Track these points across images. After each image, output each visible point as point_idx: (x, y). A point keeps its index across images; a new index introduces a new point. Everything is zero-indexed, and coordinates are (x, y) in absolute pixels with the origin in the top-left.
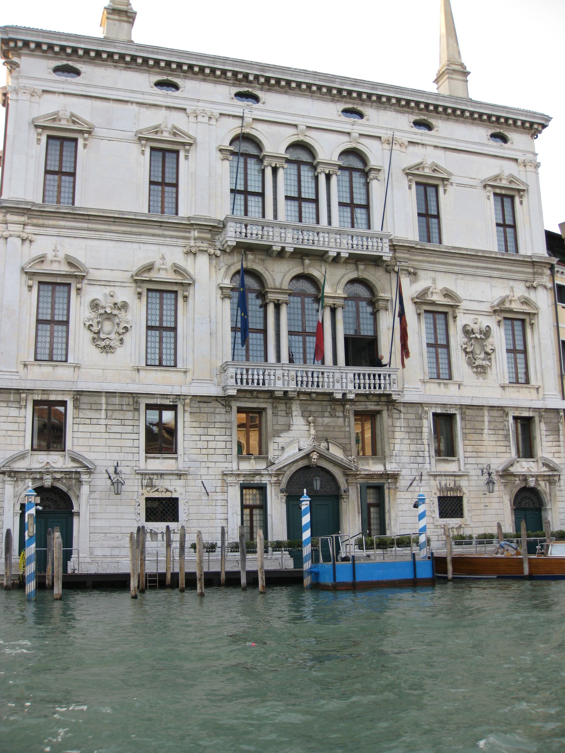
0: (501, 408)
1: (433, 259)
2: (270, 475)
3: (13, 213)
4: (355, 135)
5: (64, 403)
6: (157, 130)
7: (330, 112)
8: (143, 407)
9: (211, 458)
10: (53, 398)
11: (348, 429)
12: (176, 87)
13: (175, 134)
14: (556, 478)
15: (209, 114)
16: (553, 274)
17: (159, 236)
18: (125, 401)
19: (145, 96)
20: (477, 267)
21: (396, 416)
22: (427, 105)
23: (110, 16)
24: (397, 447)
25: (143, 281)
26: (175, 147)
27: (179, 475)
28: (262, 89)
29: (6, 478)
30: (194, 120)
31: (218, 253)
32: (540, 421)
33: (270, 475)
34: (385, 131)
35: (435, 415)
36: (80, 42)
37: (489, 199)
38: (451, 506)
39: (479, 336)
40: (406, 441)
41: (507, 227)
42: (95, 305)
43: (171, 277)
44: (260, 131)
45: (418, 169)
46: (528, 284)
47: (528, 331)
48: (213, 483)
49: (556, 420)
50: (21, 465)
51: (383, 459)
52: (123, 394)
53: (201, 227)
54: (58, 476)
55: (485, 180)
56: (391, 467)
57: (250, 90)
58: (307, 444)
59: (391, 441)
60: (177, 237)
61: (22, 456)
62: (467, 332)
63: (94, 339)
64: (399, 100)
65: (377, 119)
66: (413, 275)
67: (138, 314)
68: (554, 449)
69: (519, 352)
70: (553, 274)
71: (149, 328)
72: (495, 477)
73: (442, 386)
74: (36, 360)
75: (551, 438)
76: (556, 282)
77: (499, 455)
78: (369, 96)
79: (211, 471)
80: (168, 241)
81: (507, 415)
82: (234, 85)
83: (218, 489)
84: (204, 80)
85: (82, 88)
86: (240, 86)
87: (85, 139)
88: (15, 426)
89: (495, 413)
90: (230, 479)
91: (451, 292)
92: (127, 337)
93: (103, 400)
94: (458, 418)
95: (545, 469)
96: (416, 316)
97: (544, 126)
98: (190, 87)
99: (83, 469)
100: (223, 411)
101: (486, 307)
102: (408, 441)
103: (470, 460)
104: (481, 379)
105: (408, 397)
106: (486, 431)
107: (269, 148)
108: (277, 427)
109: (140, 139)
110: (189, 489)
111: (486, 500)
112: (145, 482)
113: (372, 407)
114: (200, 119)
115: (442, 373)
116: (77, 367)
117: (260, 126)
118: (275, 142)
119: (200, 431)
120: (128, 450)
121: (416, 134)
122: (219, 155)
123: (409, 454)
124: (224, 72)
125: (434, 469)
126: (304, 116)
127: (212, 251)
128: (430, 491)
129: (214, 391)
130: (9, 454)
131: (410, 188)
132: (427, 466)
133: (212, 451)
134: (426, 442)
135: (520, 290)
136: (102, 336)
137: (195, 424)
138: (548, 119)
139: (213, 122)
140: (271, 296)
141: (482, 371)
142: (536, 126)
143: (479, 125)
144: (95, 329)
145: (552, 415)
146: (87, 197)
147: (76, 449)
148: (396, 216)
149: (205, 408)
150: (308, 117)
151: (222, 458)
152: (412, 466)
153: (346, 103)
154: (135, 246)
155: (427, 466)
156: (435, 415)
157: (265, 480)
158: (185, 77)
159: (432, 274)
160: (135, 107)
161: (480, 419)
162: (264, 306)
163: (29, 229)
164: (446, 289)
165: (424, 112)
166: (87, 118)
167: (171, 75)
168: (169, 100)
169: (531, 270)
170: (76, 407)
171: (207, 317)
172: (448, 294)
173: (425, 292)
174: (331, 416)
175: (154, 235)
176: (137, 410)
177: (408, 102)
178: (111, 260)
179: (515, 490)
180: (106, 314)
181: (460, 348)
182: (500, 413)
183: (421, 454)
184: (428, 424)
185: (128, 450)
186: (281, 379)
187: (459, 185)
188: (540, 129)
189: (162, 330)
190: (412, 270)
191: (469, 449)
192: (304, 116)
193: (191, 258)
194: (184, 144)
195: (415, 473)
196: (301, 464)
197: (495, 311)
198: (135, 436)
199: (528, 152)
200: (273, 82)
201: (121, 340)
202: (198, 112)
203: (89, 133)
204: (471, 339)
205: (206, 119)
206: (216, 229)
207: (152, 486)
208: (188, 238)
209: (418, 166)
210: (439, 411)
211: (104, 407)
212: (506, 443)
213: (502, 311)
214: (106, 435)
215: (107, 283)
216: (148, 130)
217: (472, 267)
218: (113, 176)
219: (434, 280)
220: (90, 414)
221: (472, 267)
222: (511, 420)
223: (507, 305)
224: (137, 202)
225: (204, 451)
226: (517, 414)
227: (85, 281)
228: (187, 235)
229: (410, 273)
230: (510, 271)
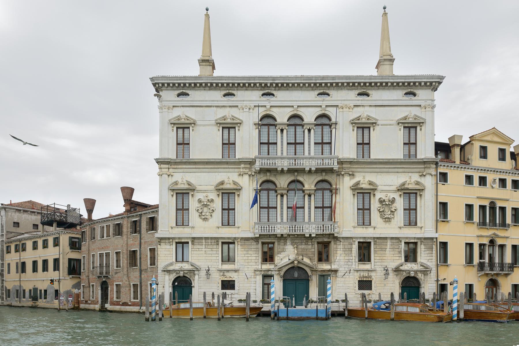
1: (363, 166)
2: (276, 271)
3: (163, 164)
4: (324, 106)
5: (188, 243)
6: (224, 118)
8: (220, 244)
9: (250, 264)
10: (183, 241)
11: (313, 250)
12: (233, 95)
13: (233, 119)
14: (429, 272)
15: (249, 107)
16: (437, 168)
17: (226, 168)
18: (213, 241)
19: (219, 102)
20: (389, 168)
21: (338, 243)
22: (365, 83)
23: (201, 64)
24: (338, 258)
25: (220, 189)
26: (234, 126)
27: (236, 271)
28: (275, 90)
29: (166, 273)
30: (242, 111)
31: (253, 173)
32: (421, 244)
33: (276, 271)
34: (340, 102)
35: (359, 242)
36: (186, 80)
37: (400, 130)
38: (365, 284)
39: (387, 203)
40: (343, 255)
41: (410, 144)
42: (200, 201)
43: (232, 186)
44: (275, 112)
45: (359, 120)
46: (420, 174)
47: (418, 198)
48: (250, 274)
49: (431, 243)
50: (171, 268)
51: (330, 264)
52: (212, 238)
53: (245, 163)
54: (186, 272)
55: (398, 120)
56: (334, 267)
57: (269, 91)
58: (292, 257)
59: (335, 255)
60: (235, 168)
61: (171, 264)
62: (381, 201)
63: (200, 215)
64: (348, 83)
65: (337, 96)
66: (352, 175)
67: (218, 204)
68: (428, 258)
70: (437, 168)
71: (223, 209)
72: (390, 271)
73: (364, 229)
74: (176, 225)
75: (427, 252)
76: (438, 171)
77: (395, 261)
78: (332, 84)
79: (249, 269)
80: (231, 170)
81: (401, 241)
82: (261, 90)
83: (252, 277)
84: (246, 90)
85: (190, 102)
86: (264, 90)
87: (193, 127)
88: (169, 253)
89: (394, 241)
90: (257, 273)
91: (372, 182)
92: (213, 214)
93: (204, 241)
94: (372, 244)
95: (422, 267)
96: (352, 196)
97: (440, 83)
98: (241, 95)
99: (195, 270)
100: (255, 243)
101: (394, 188)
102: (344, 255)
103: (377, 264)
104: (387, 224)
105: (344, 235)
106: (388, 250)
107: (279, 120)
108: (280, 250)
109: (217, 123)
110: (239, 276)
111: (385, 282)
112: (221, 274)
113: (326, 240)
114: (245, 110)
116: (193, 227)
117: (274, 109)
118: (282, 116)
119: (245, 252)
120: (214, 261)
121: (358, 100)
122: (255, 127)
123: (344, 261)
124: (255, 84)
125: (357, 268)
126: (296, 101)
127: (250, 173)
129: (251, 235)
130: (167, 263)
131: (353, 130)
132: (354, 266)
133: (250, 261)
134: (353, 255)
135: (415, 177)
136: (203, 214)
137: (242, 250)
138: (443, 78)
139: (251, 110)
140: (279, 192)
141: (388, 220)
142: (434, 84)
143: (397, 89)
144: (200, 211)
145: (429, 241)
146: (195, 154)
147: (193, 261)
148: (345, 145)
149: (247, 243)
150: (299, 101)
151: (254, 264)
152: (345, 266)
153: (320, 90)
154: (217, 174)
155: (354, 266)
156: (359, 242)
157: (273, 273)
158: (237, 90)
159: (364, 174)
160: (215, 108)
161: (385, 244)
162: (277, 196)
163: (171, 170)
164: (370, 181)
165: (363, 87)
166: (193, 117)
167: (230, 90)
168: (230, 102)
169: (423, 166)
170: (193, 244)
172: (371, 183)
173: (358, 183)
174: (306, 244)
175: (224, 168)
176: (218, 244)
177: (354, 83)
178: (205, 181)
179: (403, 278)
180: (205, 205)
181: (376, 209)
182: (397, 241)
183: (351, 261)
184: (355, 247)
185: (214, 261)
187: (382, 125)
188: (437, 84)
189: (228, 211)
190: (351, 173)
191: (377, 258)
192: (296, 101)
193: (241, 177)
194: (237, 123)
195: (347, 269)
196: (290, 266)
197: (398, 190)
198: (217, 255)
199: (428, 100)
200: (280, 85)
201: (211, 215)
202: (243, 107)
203: (194, 124)
204: (383, 205)
205: (248, 110)
206: (252, 163)
207: (224, 275)
208: (239, 168)
209: (358, 118)
210: (362, 240)
211: (204, 243)
212: (399, 255)
213: (402, 190)
214: (205, 255)
215: (205, 191)
216: (219, 119)
217: (387, 168)
218: (206, 143)
219: (364, 177)
220: (198, 247)
221: (387, 168)
222: (403, 244)
223: (406, 186)
225: (246, 261)
226: (407, 241)
227: (195, 191)
228: (239, 166)
229: (350, 175)
230: (410, 168)
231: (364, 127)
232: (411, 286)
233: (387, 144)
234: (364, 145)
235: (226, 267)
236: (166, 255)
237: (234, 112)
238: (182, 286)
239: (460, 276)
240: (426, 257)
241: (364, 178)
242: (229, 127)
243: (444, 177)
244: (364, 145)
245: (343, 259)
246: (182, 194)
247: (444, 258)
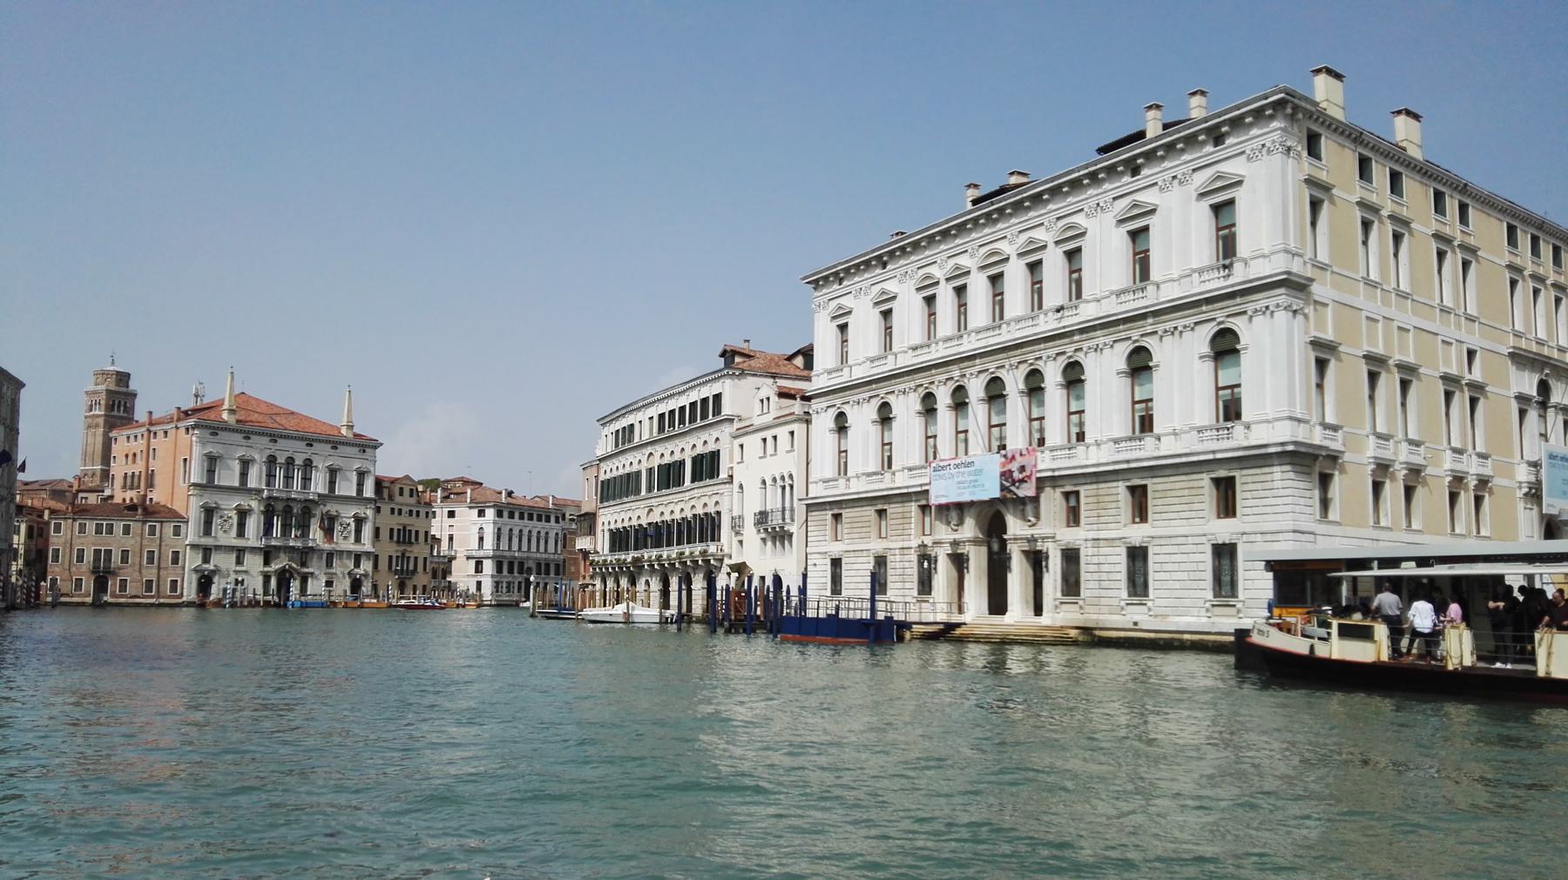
0: (349, 552)
7: (301, 445)
41: (360, 485)
44: (277, 454)
69: (358, 531)
148: (319, 485)
165: (336, 443)
178: (230, 504)
234: (332, 483)
238: (205, 583)
241: (332, 508)
242: (245, 464)
244: (332, 483)
245: (315, 567)
246: (209, 512)
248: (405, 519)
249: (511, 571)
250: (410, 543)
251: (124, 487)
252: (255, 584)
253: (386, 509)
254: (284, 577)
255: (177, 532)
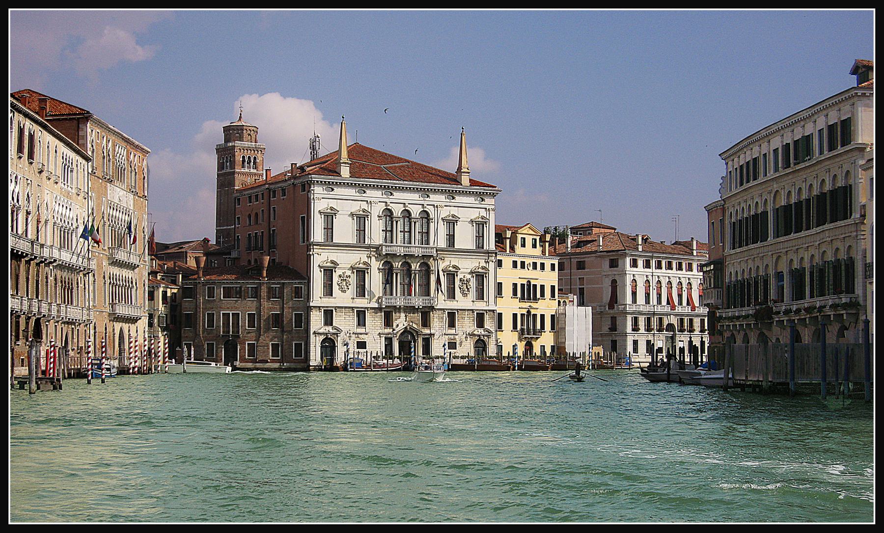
0: (473, 310)
7: (415, 196)
41: (480, 237)
44: (392, 207)
50: (321, 331)
56: (432, 332)
65: (434, 198)
115: (451, 295)
118: (397, 210)
128: (445, 340)
129: (376, 305)
135: (483, 264)
171: (375, 280)
186: (399, 301)
206: (378, 248)
224: (353, 240)
231: (451, 222)
232: (481, 345)
233: (465, 238)
235: (361, 330)
236: (316, 321)
237: (364, 206)
238: (329, 346)
239: (509, 341)
240: (489, 324)
242: (361, 219)
243: (500, 263)
245: (438, 325)
247: (500, 326)
248: (529, 273)
249: (649, 329)
250: (535, 299)
251: (249, 248)
252: (376, 346)
253: (507, 261)
254: (407, 339)
255: (297, 293)
